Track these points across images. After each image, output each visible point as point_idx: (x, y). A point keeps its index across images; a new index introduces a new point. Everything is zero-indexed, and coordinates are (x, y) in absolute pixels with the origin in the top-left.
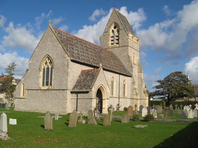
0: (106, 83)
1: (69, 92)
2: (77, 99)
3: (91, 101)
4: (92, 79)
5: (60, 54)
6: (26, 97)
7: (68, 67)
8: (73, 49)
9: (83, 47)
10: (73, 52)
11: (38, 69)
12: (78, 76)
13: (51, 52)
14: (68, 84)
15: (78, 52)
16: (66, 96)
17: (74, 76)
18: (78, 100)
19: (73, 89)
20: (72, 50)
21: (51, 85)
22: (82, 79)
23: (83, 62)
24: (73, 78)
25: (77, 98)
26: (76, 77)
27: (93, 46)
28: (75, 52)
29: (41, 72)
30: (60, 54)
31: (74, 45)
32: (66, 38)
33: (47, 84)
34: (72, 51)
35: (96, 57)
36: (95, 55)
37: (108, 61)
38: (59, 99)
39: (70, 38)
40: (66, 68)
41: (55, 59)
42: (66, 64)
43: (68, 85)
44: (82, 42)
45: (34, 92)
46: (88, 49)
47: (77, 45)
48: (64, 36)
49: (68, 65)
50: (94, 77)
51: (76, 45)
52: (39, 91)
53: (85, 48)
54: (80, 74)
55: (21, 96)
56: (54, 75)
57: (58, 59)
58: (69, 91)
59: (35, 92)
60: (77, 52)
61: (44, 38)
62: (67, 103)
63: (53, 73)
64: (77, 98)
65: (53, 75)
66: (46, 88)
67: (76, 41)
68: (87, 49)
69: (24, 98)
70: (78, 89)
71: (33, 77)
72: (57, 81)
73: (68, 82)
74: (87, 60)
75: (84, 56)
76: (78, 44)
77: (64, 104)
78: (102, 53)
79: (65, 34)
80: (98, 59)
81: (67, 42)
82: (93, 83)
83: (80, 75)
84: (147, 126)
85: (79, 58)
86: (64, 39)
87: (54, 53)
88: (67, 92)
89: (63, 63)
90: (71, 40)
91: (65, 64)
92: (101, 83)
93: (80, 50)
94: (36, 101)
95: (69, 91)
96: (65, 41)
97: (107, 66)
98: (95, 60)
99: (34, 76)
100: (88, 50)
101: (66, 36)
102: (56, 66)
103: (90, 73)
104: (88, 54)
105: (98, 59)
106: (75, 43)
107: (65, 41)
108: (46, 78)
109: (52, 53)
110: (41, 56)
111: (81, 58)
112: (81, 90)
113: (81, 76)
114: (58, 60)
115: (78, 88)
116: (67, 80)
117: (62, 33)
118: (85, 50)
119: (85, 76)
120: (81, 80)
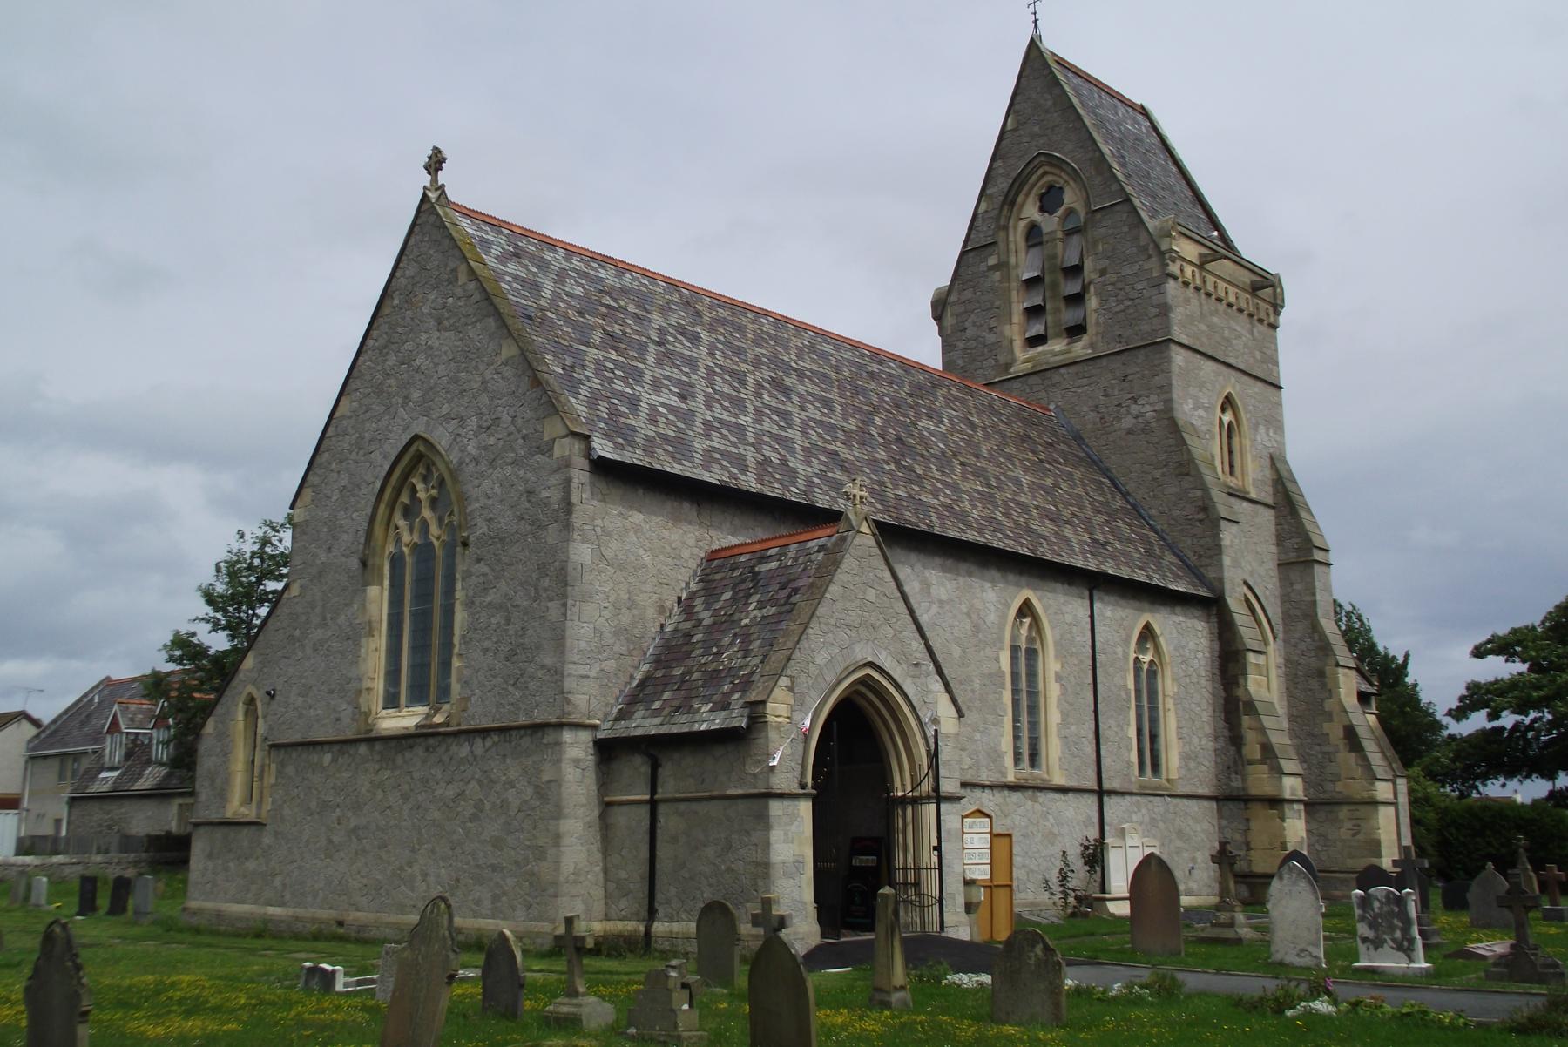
0: (917, 646)
1: (577, 748)
2: (653, 804)
3: (763, 820)
4: (778, 619)
5: (506, 418)
6: (267, 806)
7: (567, 527)
8: (635, 375)
9: (743, 367)
10: (634, 403)
11: (354, 563)
12: (671, 602)
13: (445, 409)
14: (570, 669)
15: (683, 397)
16: (557, 782)
17: (632, 605)
18: (662, 809)
19: (622, 715)
20: (619, 386)
21: (444, 692)
22: (700, 622)
23: (713, 476)
24: (626, 618)
25: (653, 791)
26: (651, 612)
27: (847, 355)
28: (647, 397)
29: (373, 591)
30: (506, 418)
31: (652, 348)
32: (579, 291)
33: (419, 694)
34: (621, 395)
35: (864, 438)
36: (852, 424)
37: (979, 473)
38: (504, 805)
39: (626, 291)
40: (552, 535)
41: (471, 467)
42: (552, 495)
43: (569, 684)
44: (741, 329)
45: (327, 758)
46: (791, 380)
47: (682, 347)
48: (561, 276)
49: (568, 507)
50: (794, 599)
51: (678, 348)
52: (363, 749)
53: (766, 373)
54: (694, 587)
55: (236, 807)
56: (469, 604)
57: (492, 464)
58: (585, 737)
59: (334, 760)
60: (674, 401)
61: (396, 302)
62: (566, 841)
63: (459, 586)
64: (653, 791)
65: (458, 608)
66: (406, 719)
67: (678, 317)
68: (776, 383)
69: (252, 817)
70: (656, 713)
71: (318, 634)
72: (485, 651)
73: (572, 655)
74: (764, 463)
75: (741, 429)
76: (695, 339)
77: (540, 854)
78: (933, 414)
79: (576, 264)
80: (881, 454)
81: (590, 319)
82: (777, 657)
83: (693, 596)
84: (986, 979)
85: (680, 446)
86: (556, 297)
87: (462, 420)
88: (558, 743)
89: (530, 492)
90: (632, 308)
91: (545, 503)
92: (863, 653)
93: (701, 387)
94: (336, 839)
95: (585, 737)
96: (567, 319)
97: (962, 517)
98: (844, 466)
99: (324, 624)
100: (786, 391)
101: (586, 276)
102: (482, 528)
103: (774, 565)
104: (785, 415)
105: (881, 454)
106: (661, 331)
107: (567, 319)
108: (414, 632)
109: (447, 418)
110: (377, 456)
111: (700, 445)
112: (681, 725)
113: (699, 601)
114: (497, 473)
115: (657, 705)
116: (559, 641)
117: (548, 255)
118: (759, 385)
119: (727, 595)
120: (688, 635)
